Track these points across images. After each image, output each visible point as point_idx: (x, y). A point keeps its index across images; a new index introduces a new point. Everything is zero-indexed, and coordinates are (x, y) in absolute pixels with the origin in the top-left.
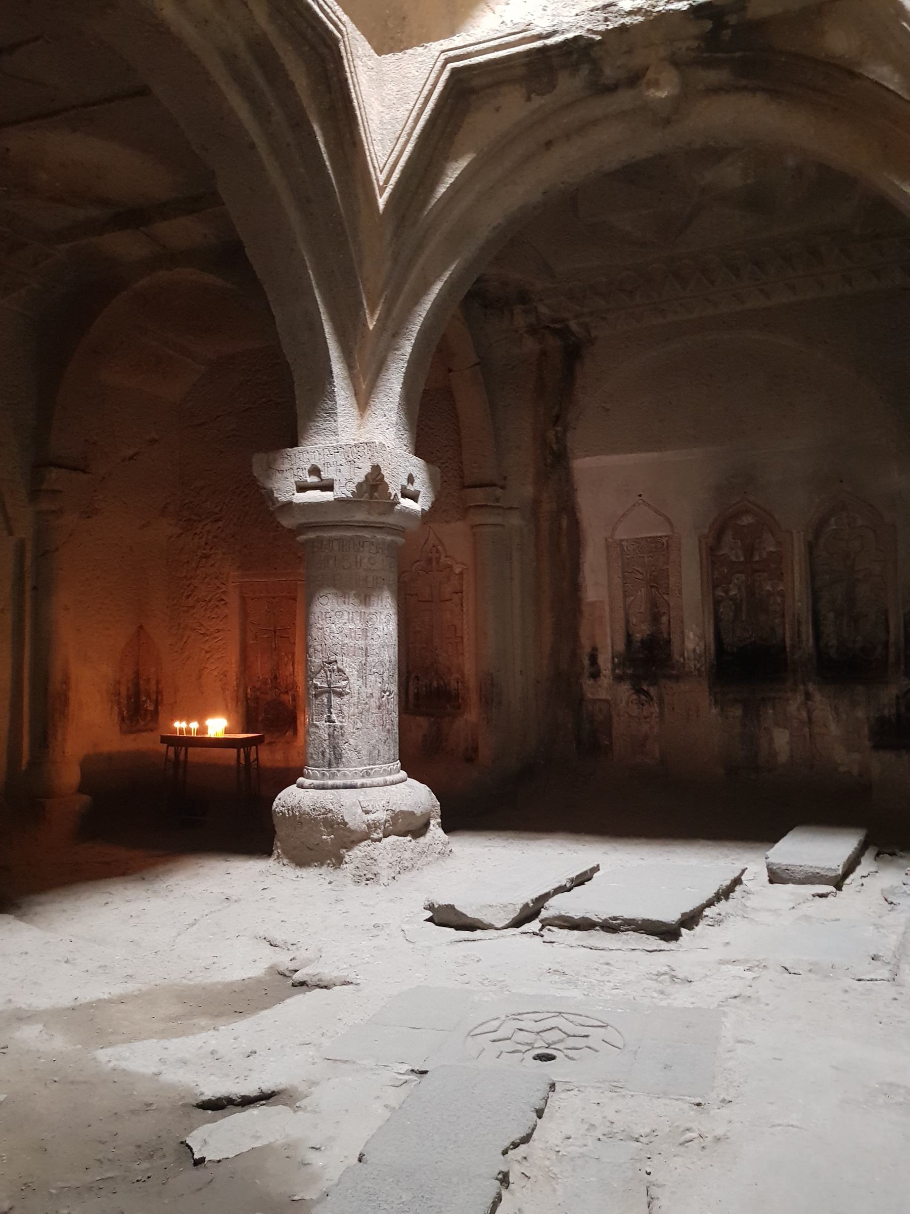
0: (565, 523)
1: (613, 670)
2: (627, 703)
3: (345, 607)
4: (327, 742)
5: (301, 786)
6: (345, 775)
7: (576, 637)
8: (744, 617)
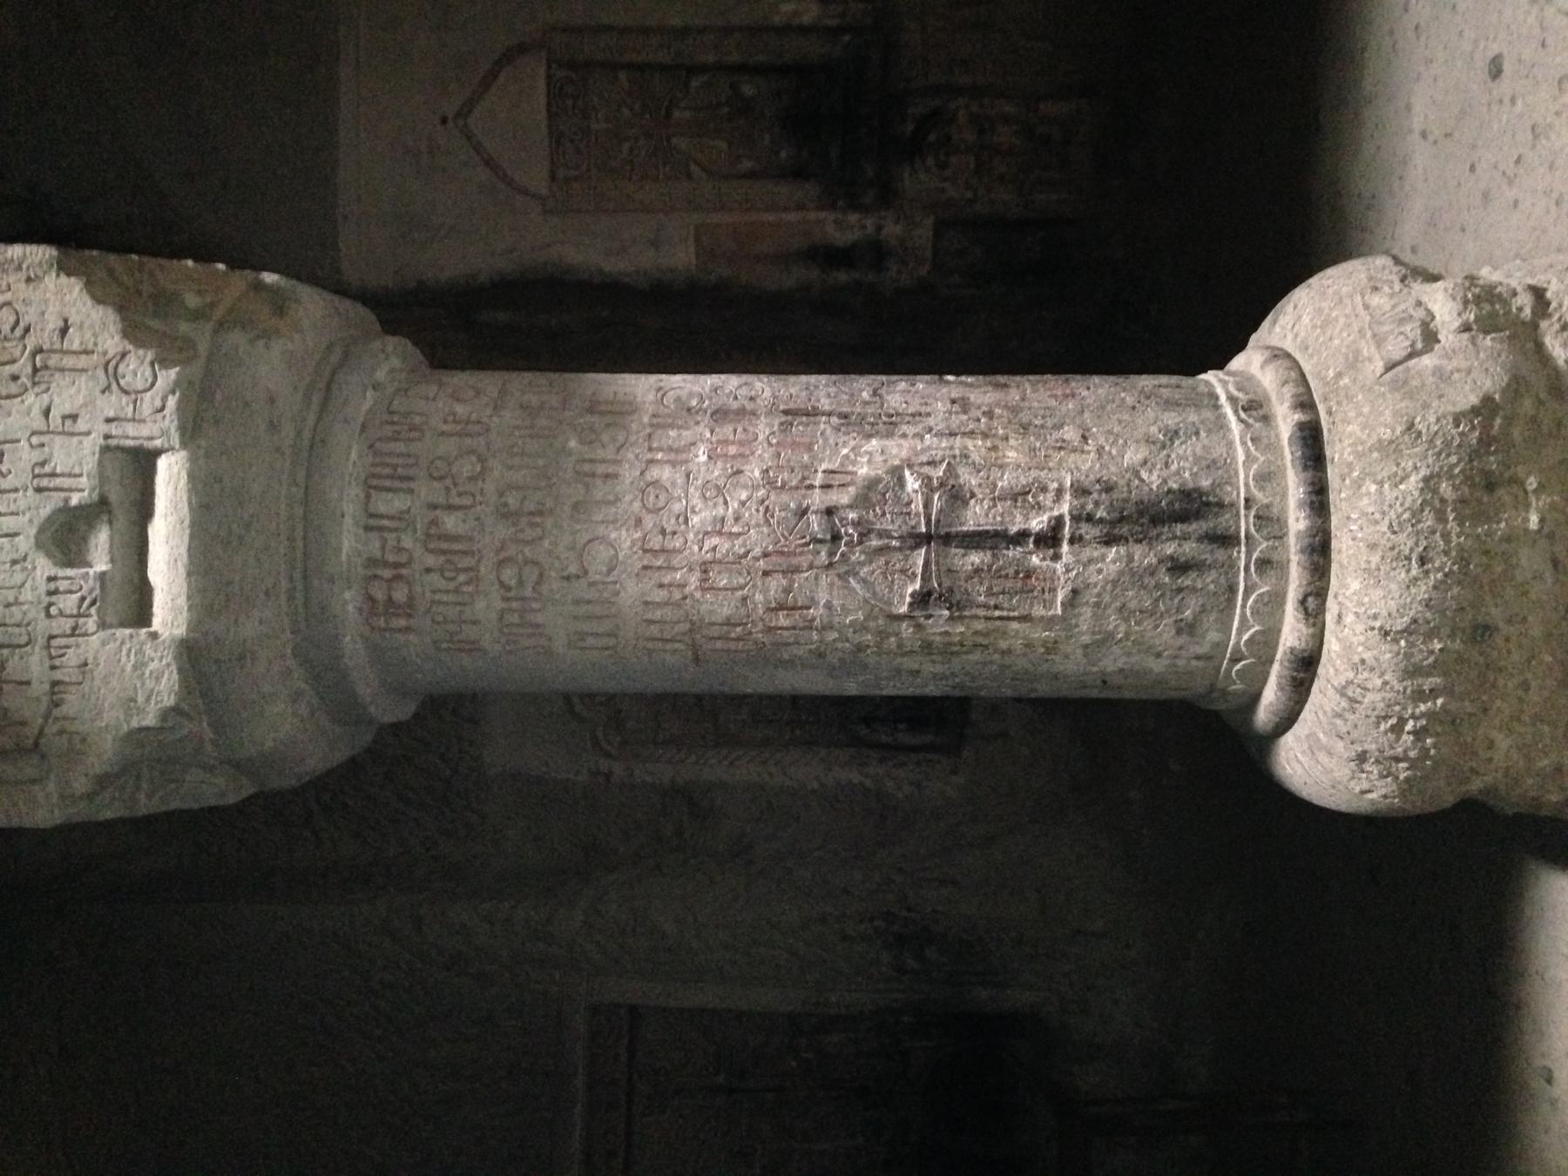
2: (946, 179)
3: (629, 474)
4: (1138, 551)
5: (1307, 664)
6: (1264, 478)
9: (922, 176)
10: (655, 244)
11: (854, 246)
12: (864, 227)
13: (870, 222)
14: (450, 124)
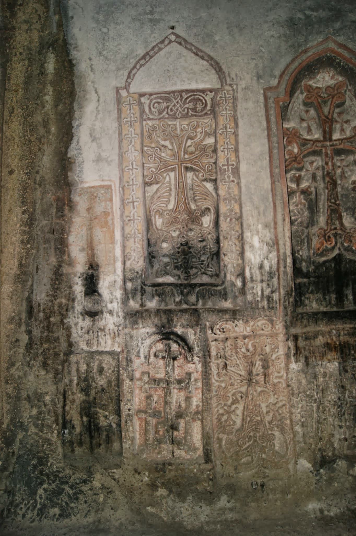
0: (51, 67)
1: (125, 301)
2: (147, 357)
7: (61, 246)
8: (322, 220)
9: (148, 342)
10: (99, 160)
11: (99, 295)
12: (111, 302)
13: (115, 306)
14: (171, 31)
